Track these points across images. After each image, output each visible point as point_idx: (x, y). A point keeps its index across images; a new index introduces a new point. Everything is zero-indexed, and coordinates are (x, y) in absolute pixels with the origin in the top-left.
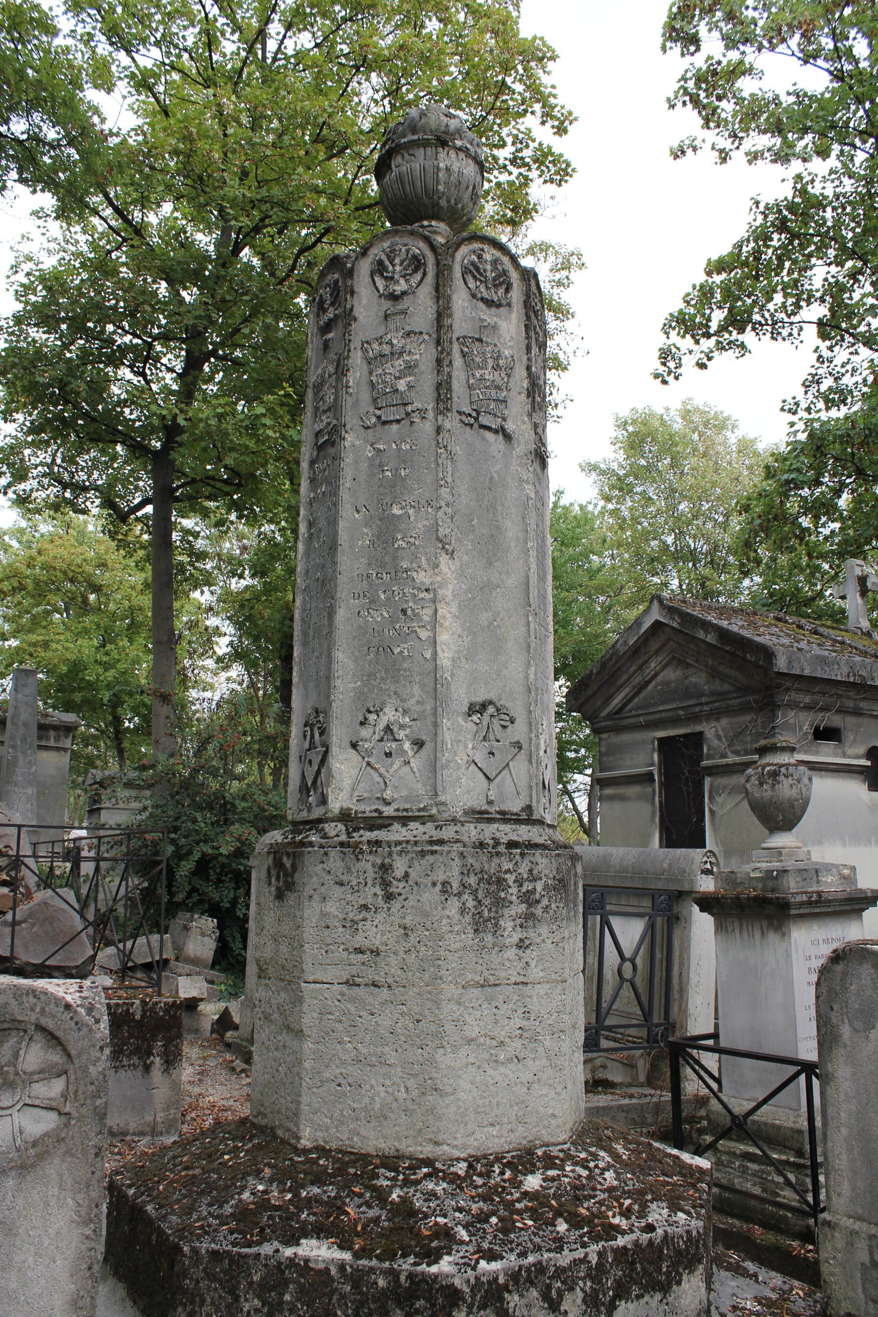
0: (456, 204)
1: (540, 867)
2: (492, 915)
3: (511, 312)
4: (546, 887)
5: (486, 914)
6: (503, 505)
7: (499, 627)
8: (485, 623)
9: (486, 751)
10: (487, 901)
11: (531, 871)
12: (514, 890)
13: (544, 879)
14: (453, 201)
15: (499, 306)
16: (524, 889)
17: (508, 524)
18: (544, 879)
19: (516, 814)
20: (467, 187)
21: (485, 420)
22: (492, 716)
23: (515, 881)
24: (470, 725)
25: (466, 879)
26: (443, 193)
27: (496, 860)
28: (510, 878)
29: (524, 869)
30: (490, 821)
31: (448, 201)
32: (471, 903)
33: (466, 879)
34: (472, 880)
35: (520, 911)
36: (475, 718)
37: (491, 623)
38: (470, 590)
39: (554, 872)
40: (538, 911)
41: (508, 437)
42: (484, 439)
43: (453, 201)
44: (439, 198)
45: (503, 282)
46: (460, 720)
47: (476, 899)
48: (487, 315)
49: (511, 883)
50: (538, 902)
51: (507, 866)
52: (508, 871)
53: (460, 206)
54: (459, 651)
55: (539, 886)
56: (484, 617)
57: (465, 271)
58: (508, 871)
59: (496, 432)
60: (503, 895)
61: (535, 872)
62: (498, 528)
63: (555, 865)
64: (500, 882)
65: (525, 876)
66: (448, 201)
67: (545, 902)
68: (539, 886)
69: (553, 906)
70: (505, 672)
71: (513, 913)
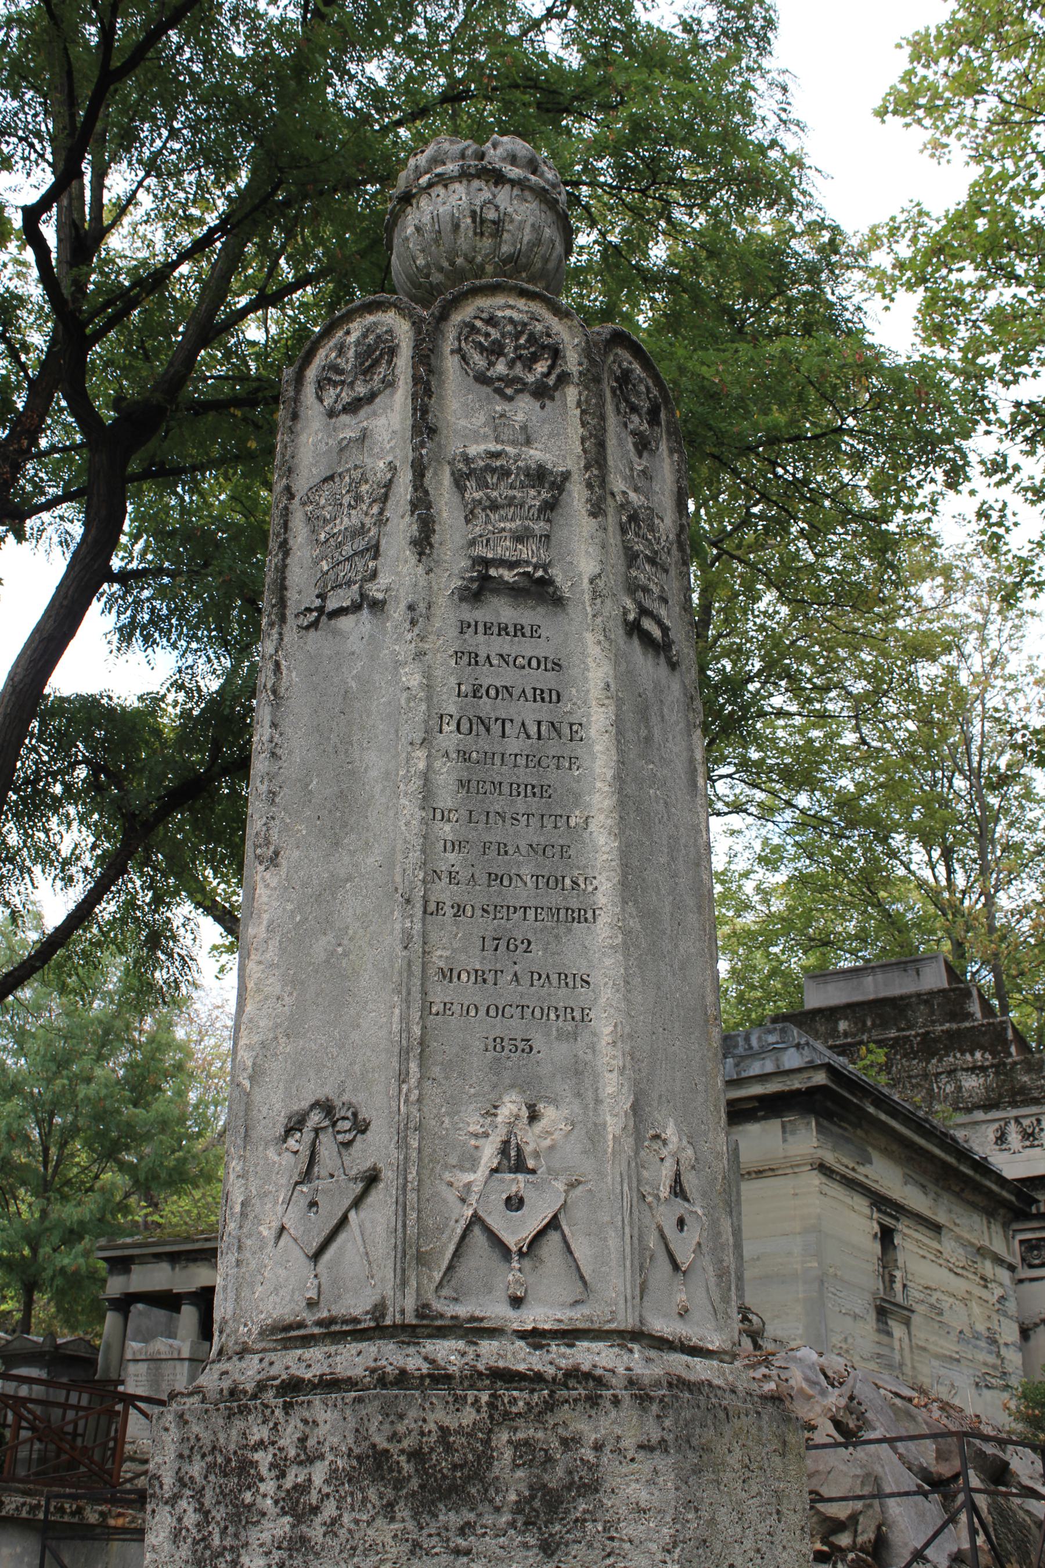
0: (452, 264)
1: (322, 1430)
2: (227, 1543)
3: (392, 394)
4: (333, 1476)
5: (216, 1542)
6: (362, 728)
7: (345, 954)
8: (323, 956)
9: (304, 1203)
10: (219, 1514)
11: (303, 1440)
12: (268, 1487)
13: (330, 1457)
14: (446, 264)
15: (372, 397)
16: (288, 1483)
17: (372, 757)
18: (330, 1457)
19: (356, 1320)
20: (456, 227)
21: (332, 605)
22: (317, 1131)
23: (273, 1466)
24: (287, 1158)
25: (186, 1467)
26: (428, 265)
27: (239, 1424)
28: (263, 1459)
29: (288, 1440)
30: (307, 1341)
31: (441, 269)
32: (191, 1519)
33: (186, 1467)
34: (196, 1469)
35: (279, 1533)
36: (291, 1142)
37: (333, 953)
38: (299, 908)
39: (350, 1440)
40: (316, 1532)
41: (377, 606)
42: (336, 633)
43: (446, 264)
44: (427, 276)
45: (381, 355)
46: (271, 1154)
47: (200, 1509)
48: (348, 427)
49: (264, 1471)
50: (315, 1510)
51: (259, 1432)
52: (261, 1445)
53: (459, 261)
54: (277, 1026)
55: (319, 1473)
56: (320, 946)
57: (321, 386)
58: (261, 1445)
59: (355, 608)
60: (248, 1497)
61: (311, 1443)
62: (352, 773)
63: (352, 1424)
64: (246, 1467)
65: (292, 1453)
66: (441, 269)
67: (330, 1510)
68: (319, 1473)
69: (346, 1519)
70: (355, 1036)
71: (266, 1536)
